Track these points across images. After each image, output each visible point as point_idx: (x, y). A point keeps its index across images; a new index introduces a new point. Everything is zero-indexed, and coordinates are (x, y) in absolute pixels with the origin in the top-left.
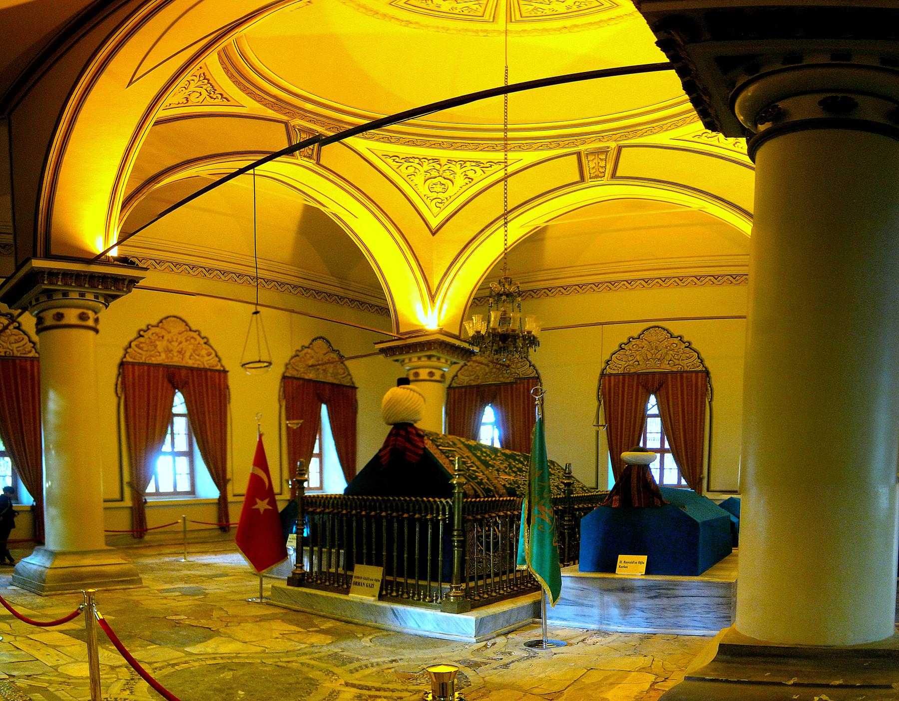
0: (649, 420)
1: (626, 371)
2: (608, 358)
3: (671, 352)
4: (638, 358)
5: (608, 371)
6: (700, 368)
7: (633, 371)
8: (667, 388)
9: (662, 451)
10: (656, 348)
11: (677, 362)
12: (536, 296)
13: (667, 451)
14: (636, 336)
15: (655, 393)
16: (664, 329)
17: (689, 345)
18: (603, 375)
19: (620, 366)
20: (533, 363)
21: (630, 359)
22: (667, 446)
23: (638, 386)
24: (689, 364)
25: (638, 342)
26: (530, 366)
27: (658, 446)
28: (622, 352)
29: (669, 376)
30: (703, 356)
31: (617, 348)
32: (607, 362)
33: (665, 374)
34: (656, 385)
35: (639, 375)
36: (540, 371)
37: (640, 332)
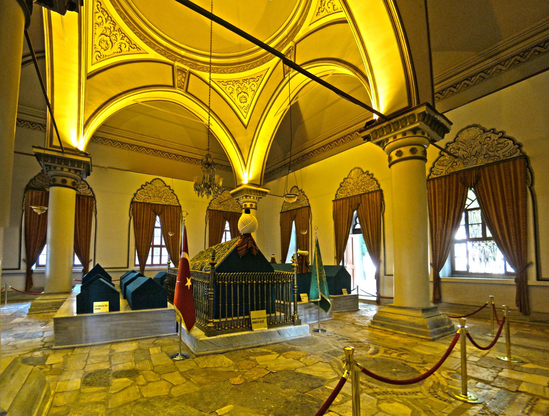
0: (155, 229)
1: (144, 201)
2: (135, 192)
3: (165, 194)
4: (150, 195)
5: (135, 200)
6: (177, 205)
7: (148, 202)
8: (164, 213)
9: (161, 246)
10: (159, 190)
11: (168, 200)
12: (95, 141)
13: (163, 246)
14: (149, 182)
15: (159, 216)
16: (162, 181)
17: (173, 192)
18: (132, 202)
19: (141, 199)
20: (91, 186)
21: (147, 194)
22: (164, 244)
23: (151, 211)
24: (173, 202)
25: (150, 186)
26: (88, 188)
27: (159, 244)
28: (142, 190)
29: (165, 207)
30: (179, 198)
31: (140, 187)
32: (135, 195)
33: (163, 205)
34: (160, 211)
35: (152, 204)
36: (95, 193)
37: (151, 180)
